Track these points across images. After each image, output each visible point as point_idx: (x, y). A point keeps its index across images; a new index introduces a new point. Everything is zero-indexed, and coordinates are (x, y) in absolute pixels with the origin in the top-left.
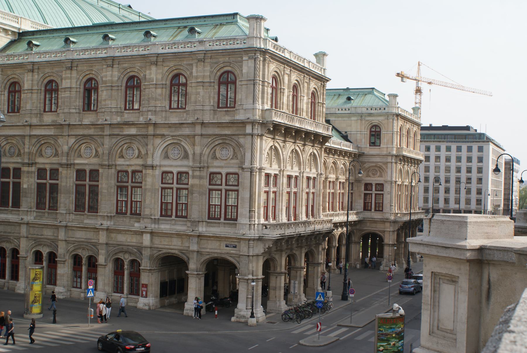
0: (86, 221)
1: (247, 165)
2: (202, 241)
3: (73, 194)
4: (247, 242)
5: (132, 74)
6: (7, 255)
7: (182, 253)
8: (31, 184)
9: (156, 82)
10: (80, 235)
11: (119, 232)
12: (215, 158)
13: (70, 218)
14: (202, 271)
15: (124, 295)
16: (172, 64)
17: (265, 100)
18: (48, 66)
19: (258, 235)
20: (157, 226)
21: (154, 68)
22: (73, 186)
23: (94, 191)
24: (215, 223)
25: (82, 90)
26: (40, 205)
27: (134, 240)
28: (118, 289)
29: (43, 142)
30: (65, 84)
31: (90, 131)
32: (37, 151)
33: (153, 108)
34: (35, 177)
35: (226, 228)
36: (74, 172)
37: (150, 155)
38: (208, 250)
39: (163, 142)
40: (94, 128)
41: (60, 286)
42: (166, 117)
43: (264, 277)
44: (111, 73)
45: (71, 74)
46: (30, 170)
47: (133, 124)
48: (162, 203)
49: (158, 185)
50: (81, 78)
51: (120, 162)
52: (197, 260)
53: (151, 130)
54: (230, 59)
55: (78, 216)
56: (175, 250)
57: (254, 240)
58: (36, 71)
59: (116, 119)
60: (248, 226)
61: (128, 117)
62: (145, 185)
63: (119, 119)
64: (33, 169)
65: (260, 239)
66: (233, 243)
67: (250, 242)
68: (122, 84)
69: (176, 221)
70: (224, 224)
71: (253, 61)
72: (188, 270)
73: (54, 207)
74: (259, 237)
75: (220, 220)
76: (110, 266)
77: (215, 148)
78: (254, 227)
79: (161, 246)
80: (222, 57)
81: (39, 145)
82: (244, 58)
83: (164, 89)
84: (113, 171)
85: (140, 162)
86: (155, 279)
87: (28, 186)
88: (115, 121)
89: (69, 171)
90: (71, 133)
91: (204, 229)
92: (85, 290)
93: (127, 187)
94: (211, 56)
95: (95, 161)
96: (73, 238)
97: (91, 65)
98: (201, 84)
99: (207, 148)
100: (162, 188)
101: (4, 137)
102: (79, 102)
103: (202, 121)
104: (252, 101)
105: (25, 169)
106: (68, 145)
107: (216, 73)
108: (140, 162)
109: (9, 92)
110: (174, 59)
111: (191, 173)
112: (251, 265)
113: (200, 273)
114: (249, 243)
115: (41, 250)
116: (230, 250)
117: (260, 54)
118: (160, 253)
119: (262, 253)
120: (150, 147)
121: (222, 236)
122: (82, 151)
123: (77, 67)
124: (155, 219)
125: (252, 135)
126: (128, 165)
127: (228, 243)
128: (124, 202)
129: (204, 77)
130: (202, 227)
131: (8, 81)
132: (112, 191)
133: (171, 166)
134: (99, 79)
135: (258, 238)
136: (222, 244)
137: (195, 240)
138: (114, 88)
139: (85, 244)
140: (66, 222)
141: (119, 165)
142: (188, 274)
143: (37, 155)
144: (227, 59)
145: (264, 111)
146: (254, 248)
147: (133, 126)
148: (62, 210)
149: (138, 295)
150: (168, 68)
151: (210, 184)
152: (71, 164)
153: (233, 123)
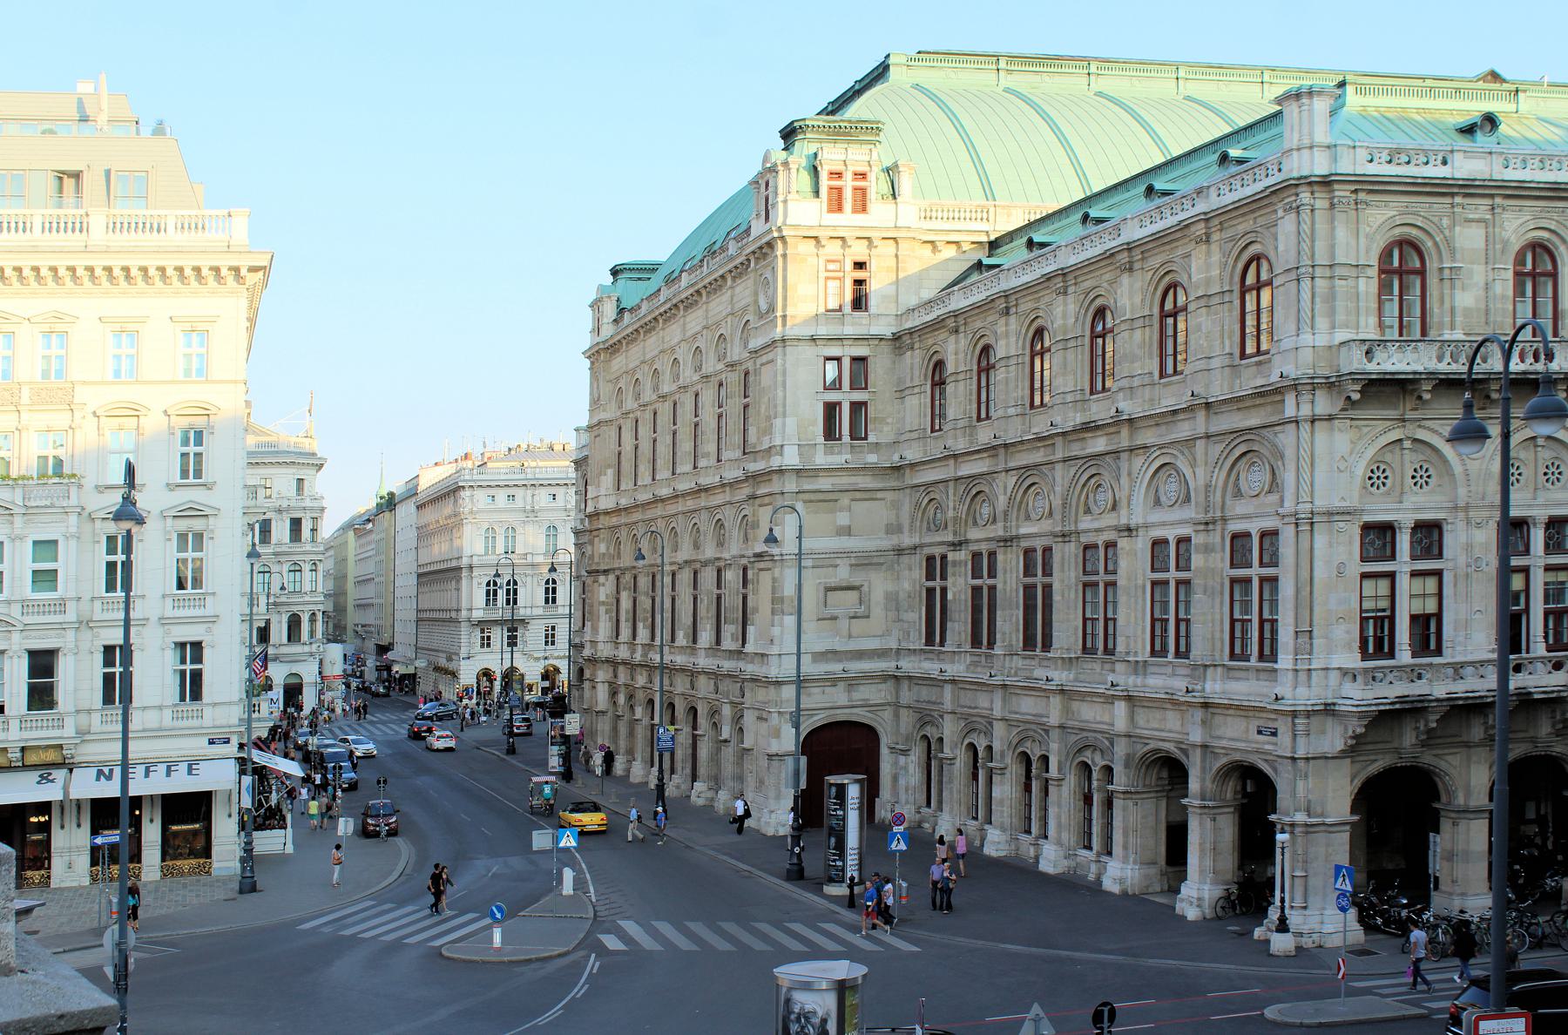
0: (1040, 673)
1: (1289, 505)
2: (1216, 717)
3: (1018, 608)
4: (1290, 719)
5: (1099, 302)
7: (1181, 749)
8: (960, 592)
9: (1132, 312)
10: (1028, 706)
12: (1238, 494)
13: (1013, 666)
14: (1221, 800)
16: (1155, 261)
17: (1340, 317)
18: (977, 314)
19: (1322, 701)
20: (1139, 681)
21: (1125, 279)
22: (1017, 590)
24: (1240, 669)
25: (1027, 359)
26: (976, 642)
27: (1106, 718)
29: (974, 492)
30: (1000, 351)
31: (1038, 455)
32: (967, 514)
33: (1125, 383)
34: (966, 575)
35: (1261, 683)
36: (1018, 557)
37: (1124, 502)
38: (1224, 743)
39: (1146, 465)
40: (1044, 446)
41: (995, 828)
42: (1152, 400)
43: (1356, 818)
44: (1061, 308)
45: (1007, 325)
46: (957, 559)
47: (1098, 427)
48: (1153, 620)
49: (1145, 575)
50: (1024, 331)
51: (1086, 523)
52: (1203, 769)
53: (1124, 439)
54: (1259, 220)
55: (1027, 662)
56: (1169, 741)
57: (1308, 714)
58: (962, 329)
59: (1074, 420)
60: (1290, 675)
61: (1100, 410)
63: (1079, 419)
64: (963, 555)
65: (1329, 710)
67: (1297, 721)
68: (1083, 331)
70: (1257, 670)
71: (1293, 216)
72: (1187, 796)
73: (991, 644)
74: (1325, 704)
76: (1071, 781)
77: (1239, 463)
78: (1309, 677)
79: (1146, 732)
80: (1241, 220)
81: (969, 500)
82: (1280, 213)
83: (1147, 328)
84: (1073, 544)
85: (1109, 520)
86: (1143, 817)
87: (954, 594)
88: (1069, 425)
89: (1009, 556)
90: (1012, 464)
91: (1218, 687)
92: (1037, 838)
93: (1096, 584)
94: (1221, 223)
95: (1046, 526)
96: (1016, 713)
97: (1036, 296)
98: (1202, 302)
99: (1220, 469)
100: (1154, 583)
101: (923, 488)
102: (1023, 389)
103: (1204, 401)
104: (1293, 327)
105: (950, 556)
106: (1005, 494)
107: (1234, 267)
108: (1109, 520)
109: (934, 385)
110: (1162, 249)
111: (1193, 542)
112: (1300, 785)
113: (1210, 804)
114: (1294, 724)
116: (1264, 743)
117: (1312, 193)
118: (1145, 749)
119: (1342, 751)
120: (1124, 480)
122: (1030, 504)
123: (1016, 305)
124: (1137, 662)
125: (1297, 422)
126: (1097, 530)
127: (1261, 723)
129: (1208, 281)
130: (1214, 680)
131: (930, 359)
132: (1073, 595)
133: (1164, 524)
134: (1050, 329)
135: (1322, 707)
136: (1251, 727)
137: (1199, 714)
138: (1071, 344)
139: (1033, 727)
140: (1002, 674)
141: (1085, 532)
142: (1185, 807)
143: (970, 522)
144: (1251, 222)
145: (1334, 350)
146: (1312, 737)
147: (1100, 433)
148: (998, 651)
150: (1151, 273)
151: (1232, 565)
152: (1011, 539)
153: (1261, 395)
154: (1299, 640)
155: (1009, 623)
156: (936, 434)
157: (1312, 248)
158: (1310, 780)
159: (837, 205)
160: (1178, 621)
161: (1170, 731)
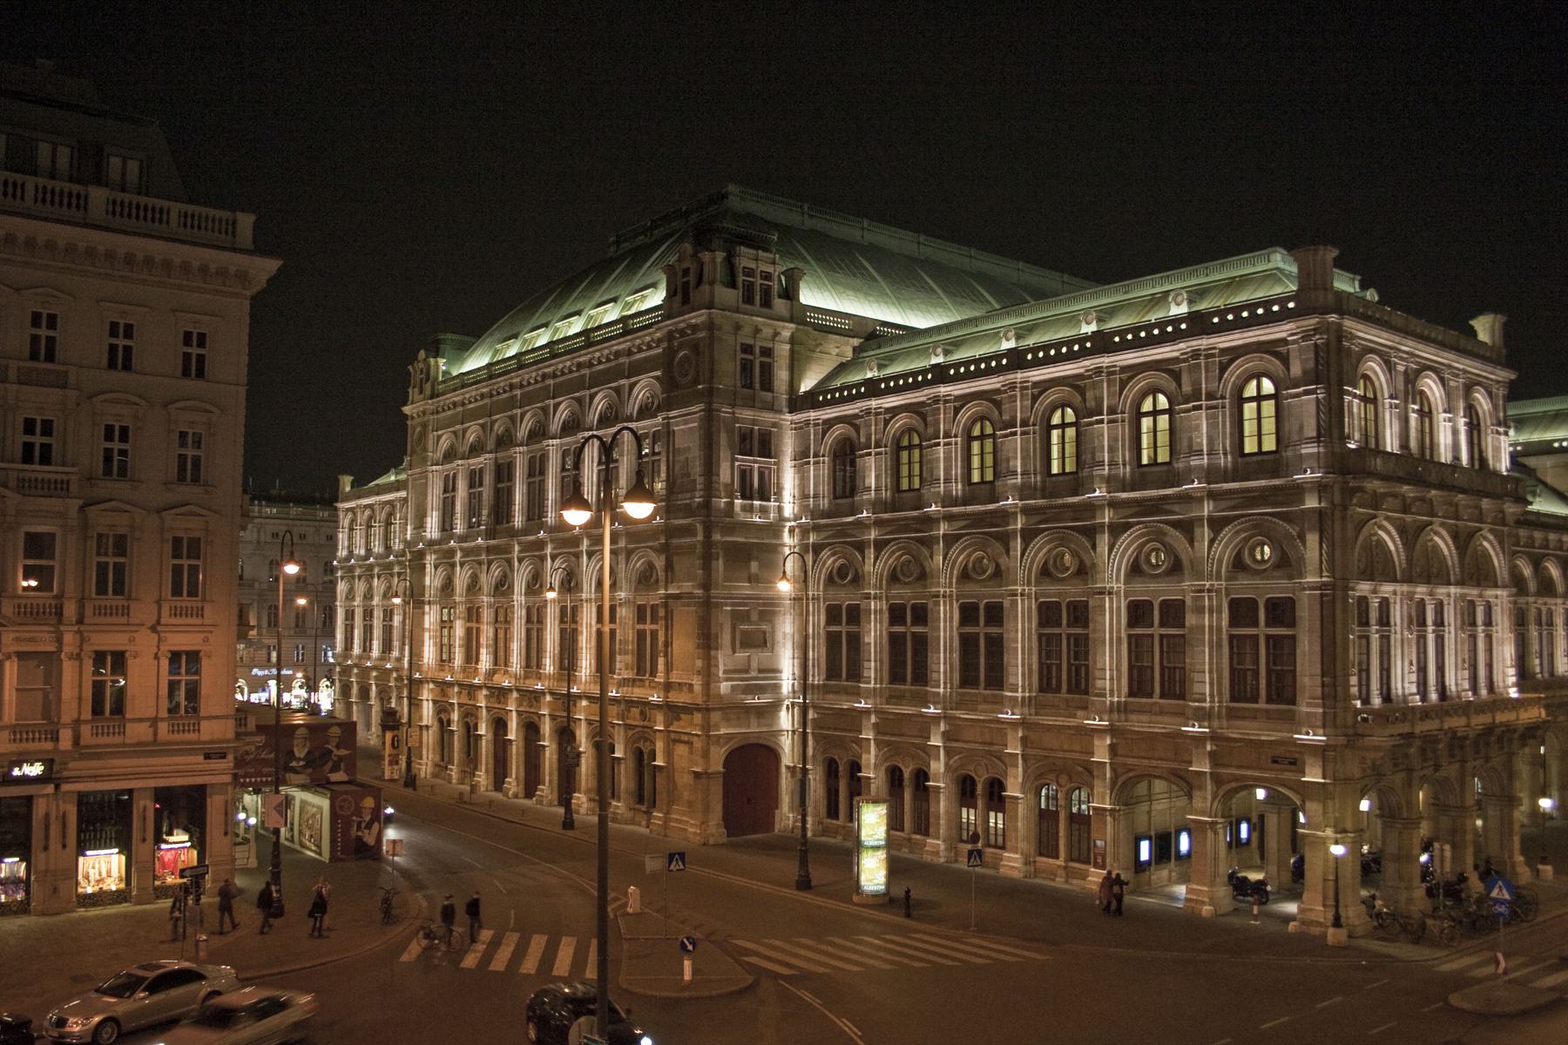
6: (841, 774)
11: (1049, 728)
15: (1061, 862)
23: (997, 646)
26: (896, 675)
27: (1077, 747)
28: (1046, 846)
57: (1334, 748)
62: (1094, 631)
66: (1288, 755)
69: (1161, 706)
70: (1267, 711)
75: (1257, 702)
76: (1031, 796)
78: (1335, 717)
96: (957, 741)
100: (1130, 636)
111: (1189, 601)
115: (900, 765)
118: (1131, 774)
121: (1263, 738)
128: (1054, 668)
136: (1263, 757)
149: (1088, 862)
154: (1326, 689)
155: (944, 664)
156: (839, 501)
157: (1328, 371)
158: (1337, 801)
159: (749, 299)
160: (1162, 668)
161: (1161, 759)
